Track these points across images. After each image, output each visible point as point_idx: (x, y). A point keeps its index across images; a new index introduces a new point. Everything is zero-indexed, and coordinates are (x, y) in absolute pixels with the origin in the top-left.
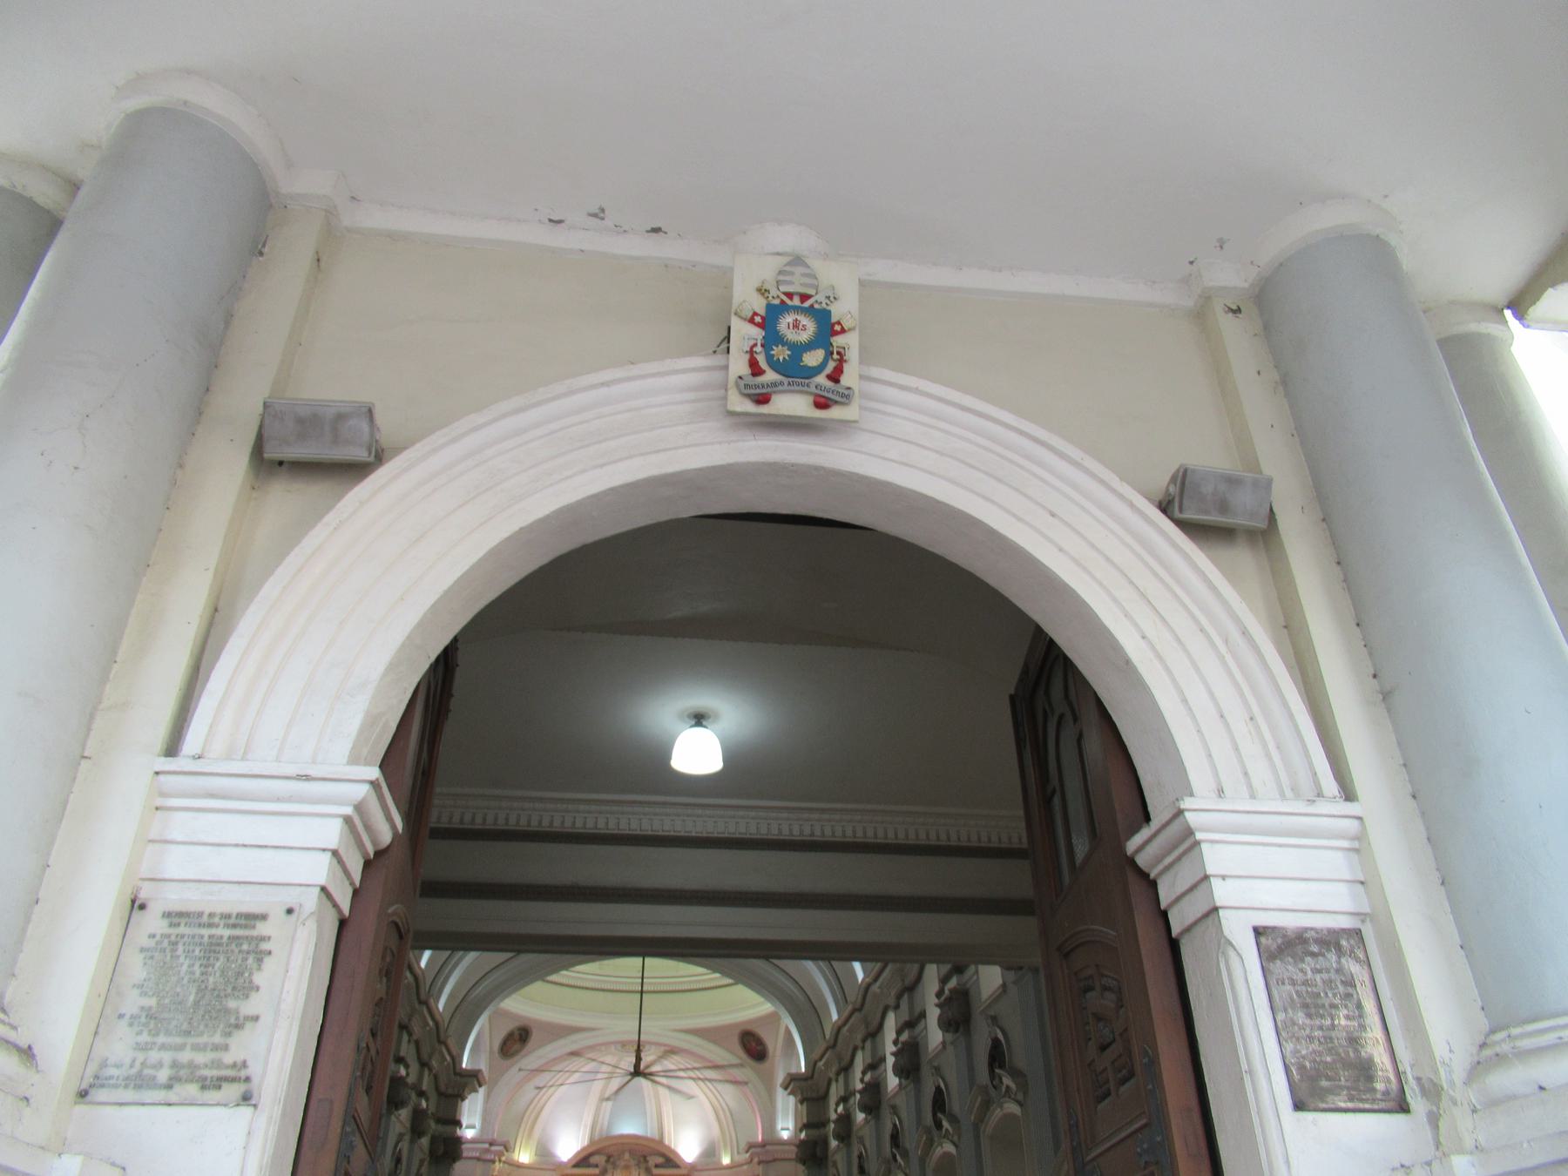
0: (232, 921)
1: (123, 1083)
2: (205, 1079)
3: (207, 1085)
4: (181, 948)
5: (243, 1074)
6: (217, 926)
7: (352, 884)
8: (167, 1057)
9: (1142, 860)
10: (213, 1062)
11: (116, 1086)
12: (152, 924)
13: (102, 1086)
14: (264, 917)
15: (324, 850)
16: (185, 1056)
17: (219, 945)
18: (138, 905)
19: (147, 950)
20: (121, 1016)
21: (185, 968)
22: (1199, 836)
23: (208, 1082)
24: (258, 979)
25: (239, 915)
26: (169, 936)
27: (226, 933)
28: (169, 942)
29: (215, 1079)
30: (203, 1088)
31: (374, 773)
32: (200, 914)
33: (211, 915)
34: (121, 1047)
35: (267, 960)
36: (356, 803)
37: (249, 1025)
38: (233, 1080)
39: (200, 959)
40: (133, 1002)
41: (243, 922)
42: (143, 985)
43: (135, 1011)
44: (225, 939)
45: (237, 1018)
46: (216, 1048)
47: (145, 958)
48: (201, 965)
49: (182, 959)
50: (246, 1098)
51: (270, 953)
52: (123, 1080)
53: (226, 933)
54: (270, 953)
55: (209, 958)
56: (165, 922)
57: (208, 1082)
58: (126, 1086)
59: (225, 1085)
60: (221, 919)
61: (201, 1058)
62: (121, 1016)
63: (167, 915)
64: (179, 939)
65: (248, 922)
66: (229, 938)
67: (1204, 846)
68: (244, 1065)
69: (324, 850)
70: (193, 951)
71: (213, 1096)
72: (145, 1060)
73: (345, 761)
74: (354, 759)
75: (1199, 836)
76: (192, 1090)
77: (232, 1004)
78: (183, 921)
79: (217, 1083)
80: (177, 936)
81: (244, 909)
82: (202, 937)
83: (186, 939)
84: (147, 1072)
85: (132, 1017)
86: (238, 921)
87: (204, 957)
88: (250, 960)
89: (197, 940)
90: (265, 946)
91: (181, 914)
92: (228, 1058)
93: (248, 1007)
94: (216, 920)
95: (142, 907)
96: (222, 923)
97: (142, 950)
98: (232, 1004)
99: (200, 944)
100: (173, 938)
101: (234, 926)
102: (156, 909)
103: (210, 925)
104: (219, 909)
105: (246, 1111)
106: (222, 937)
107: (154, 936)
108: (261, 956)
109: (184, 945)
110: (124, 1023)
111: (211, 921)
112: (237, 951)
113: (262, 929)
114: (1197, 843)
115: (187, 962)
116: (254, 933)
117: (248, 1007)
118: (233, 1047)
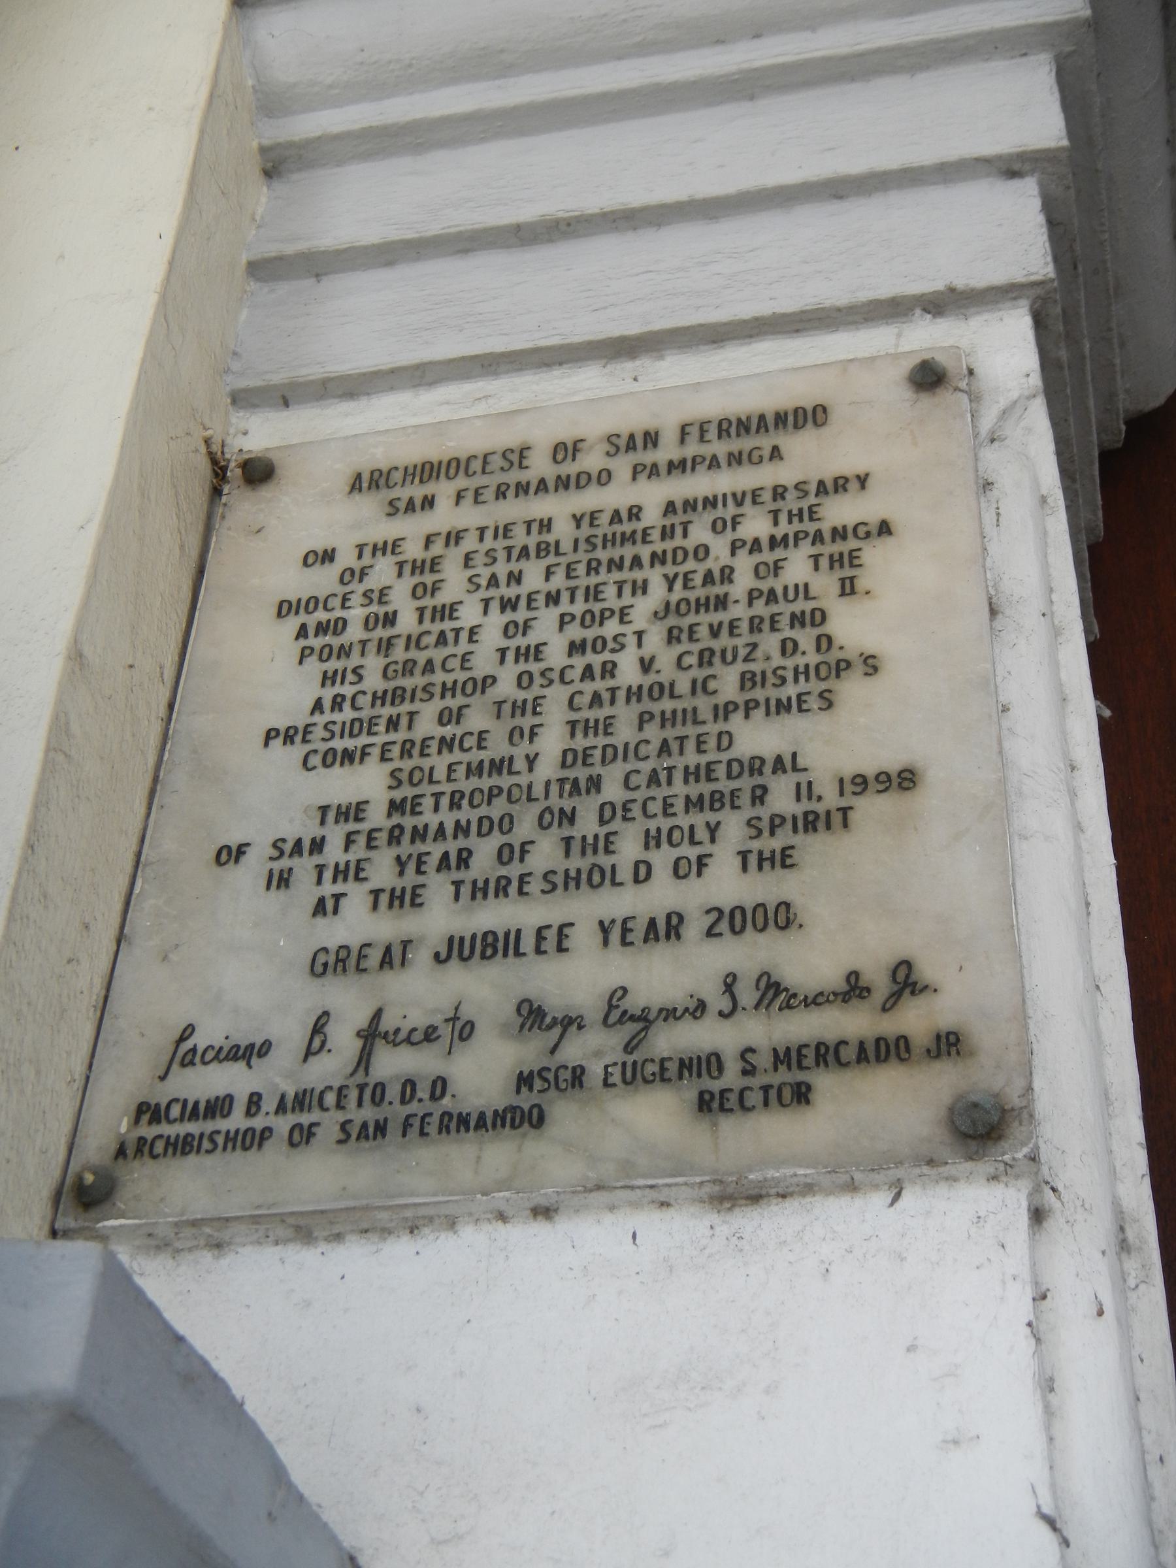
0: (668, 451)
1: (283, 1125)
2: (713, 1062)
6: (604, 478)
10: (730, 984)
11: (253, 1140)
13: (183, 1146)
19: (312, 603)
21: (492, 636)
26: (391, 547)
28: (401, 565)
29: (763, 1060)
30: (706, 1104)
32: (518, 456)
33: (566, 450)
35: (873, 554)
39: (553, 599)
41: (721, 448)
42: (307, 730)
44: (652, 517)
45: (804, 791)
47: (302, 632)
49: (469, 614)
52: (281, 1108)
54: (885, 529)
55: (593, 593)
56: (369, 505)
57: (731, 1077)
58: (302, 1136)
59: (824, 1082)
64: (437, 548)
65: (745, 444)
66: (670, 508)
70: (516, 578)
72: (378, 1014)
78: (444, 490)
80: (428, 541)
82: (546, 525)
83: (470, 543)
86: (692, 449)
87: (573, 591)
89: (519, 538)
91: (428, 471)
94: (592, 461)
97: (284, 609)
99: (542, 550)
100: (413, 550)
101: (678, 467)
103: (581, 481)
106: (635, 513)
107: (328, 556)
109: (468, 560)
112: (720, 547)
115: (496, 620)
116: (784, 474)
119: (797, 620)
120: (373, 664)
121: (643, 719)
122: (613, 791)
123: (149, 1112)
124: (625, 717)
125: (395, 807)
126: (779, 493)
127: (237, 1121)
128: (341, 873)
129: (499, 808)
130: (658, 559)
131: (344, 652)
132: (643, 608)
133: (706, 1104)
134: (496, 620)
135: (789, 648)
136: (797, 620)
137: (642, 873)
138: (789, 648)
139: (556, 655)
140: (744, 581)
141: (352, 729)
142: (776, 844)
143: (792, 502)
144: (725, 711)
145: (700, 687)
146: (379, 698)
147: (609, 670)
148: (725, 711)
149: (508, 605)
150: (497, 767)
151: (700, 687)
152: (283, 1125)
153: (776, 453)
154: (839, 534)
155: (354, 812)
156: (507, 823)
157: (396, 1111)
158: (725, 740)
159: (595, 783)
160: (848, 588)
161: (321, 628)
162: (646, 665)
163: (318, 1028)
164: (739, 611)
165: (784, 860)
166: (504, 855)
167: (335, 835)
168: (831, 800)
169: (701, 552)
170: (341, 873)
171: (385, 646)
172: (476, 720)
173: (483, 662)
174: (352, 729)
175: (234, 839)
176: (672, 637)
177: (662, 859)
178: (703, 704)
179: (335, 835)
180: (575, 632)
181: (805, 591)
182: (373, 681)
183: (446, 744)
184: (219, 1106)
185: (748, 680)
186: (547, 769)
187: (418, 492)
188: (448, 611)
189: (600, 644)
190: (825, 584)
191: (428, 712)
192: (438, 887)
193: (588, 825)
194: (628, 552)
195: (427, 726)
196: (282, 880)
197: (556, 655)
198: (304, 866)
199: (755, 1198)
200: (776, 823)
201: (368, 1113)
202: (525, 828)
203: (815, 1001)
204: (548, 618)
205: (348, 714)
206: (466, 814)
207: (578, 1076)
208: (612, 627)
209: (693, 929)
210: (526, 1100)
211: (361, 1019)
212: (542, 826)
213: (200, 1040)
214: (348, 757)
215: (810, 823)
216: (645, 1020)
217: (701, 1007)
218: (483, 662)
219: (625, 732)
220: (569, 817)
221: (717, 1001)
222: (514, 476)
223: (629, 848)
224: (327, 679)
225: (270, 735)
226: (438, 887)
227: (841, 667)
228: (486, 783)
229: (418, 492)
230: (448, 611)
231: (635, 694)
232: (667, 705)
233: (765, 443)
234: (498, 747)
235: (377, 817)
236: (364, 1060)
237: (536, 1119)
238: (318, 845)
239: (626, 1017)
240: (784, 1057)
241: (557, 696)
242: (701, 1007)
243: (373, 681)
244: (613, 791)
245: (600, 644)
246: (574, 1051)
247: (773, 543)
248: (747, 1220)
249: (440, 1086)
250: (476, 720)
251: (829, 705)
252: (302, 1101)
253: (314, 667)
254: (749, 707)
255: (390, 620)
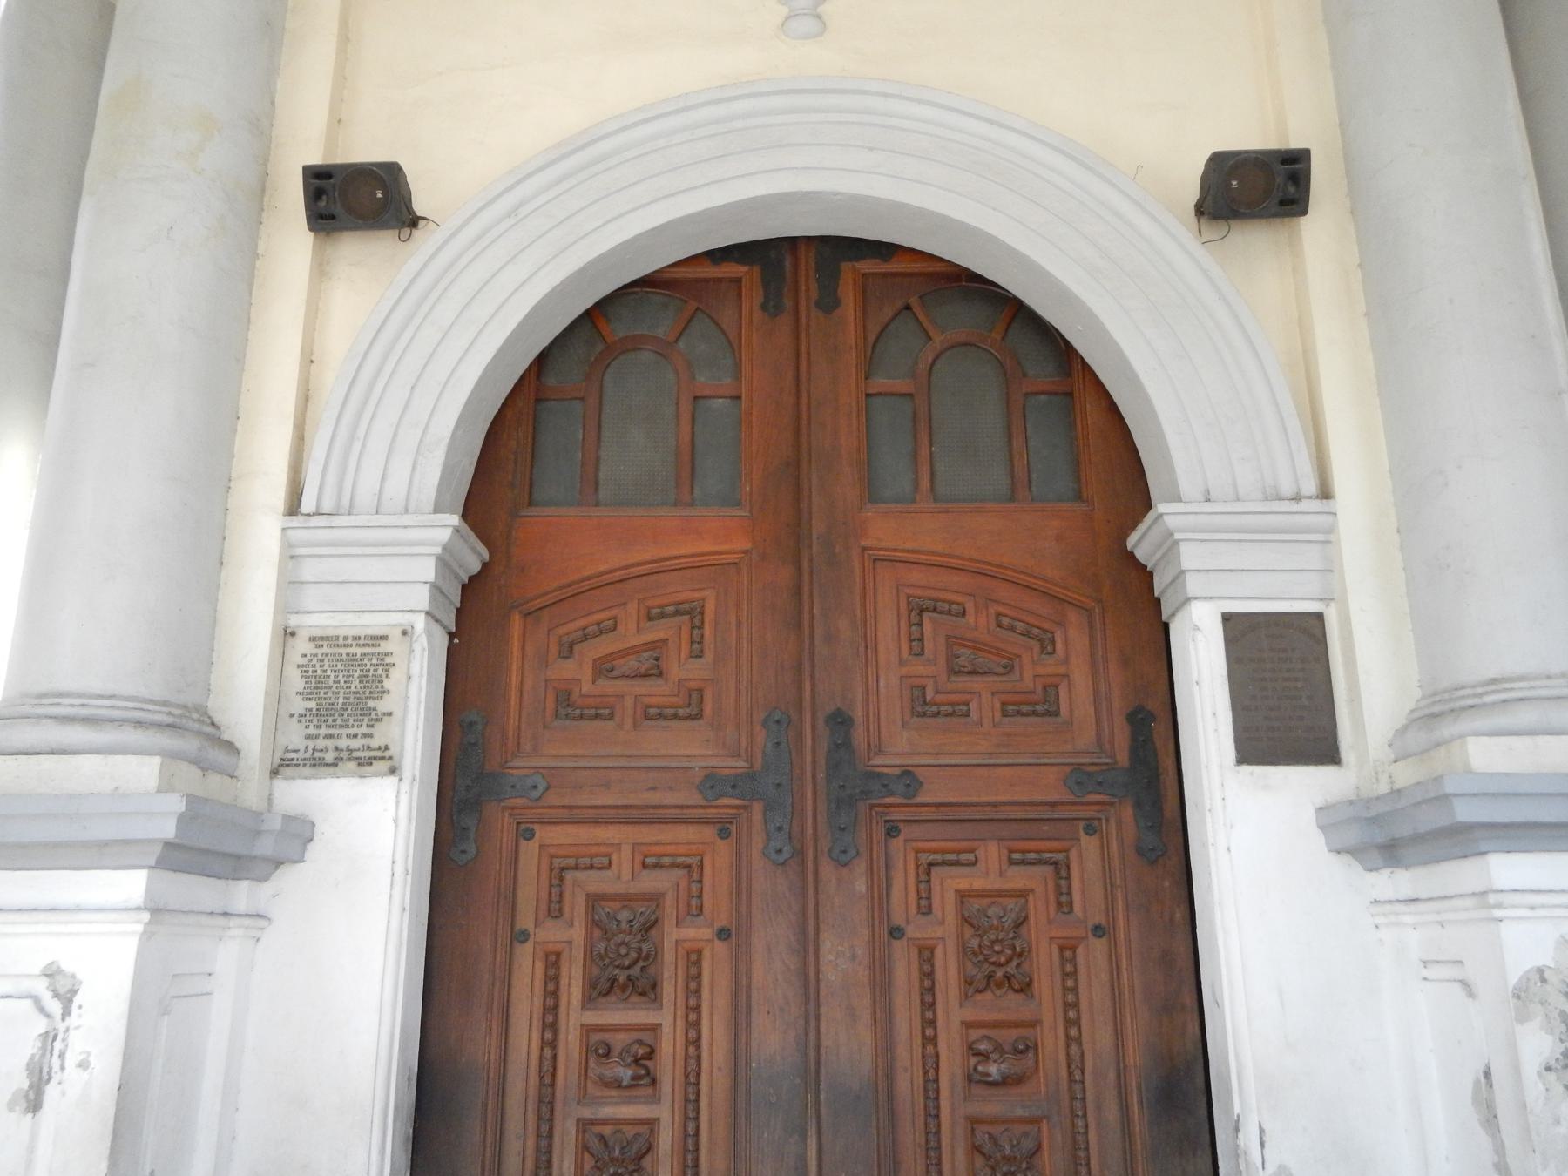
0: (362, 642)
3: (362, 763)
4: (326, 664)
5: (387, 754)
7: (451, 603)
8: (330, 743)
9: (1140, 555)
10: (363, 746)
12: (301, 646)
13: (288, 765)
14: (385, 638)
15: (426, 583)
16: (343, 743)
17: (355, 660)
18: (289, 633)
19: (303, 666)
20: (292, 716)
21: (332, 678)
22: (1177, 536)
23: (362, 761)
24: (387, 684)
25: (367, 637)
26: (316, 655)
27: (359, 651)
30: (359, 764)
31: (455, 520)
32: (337, 638)
33: (346, 638)
34: (295, 736)
35: (392, 670)
36: (443, 544)
37: (385, 718)
38: (382, 758)
39: (342, 671)
40: (299, 705)
41: (370, 642)
43: (303, 712)
44: (358, 656)
45: (376, 714)
46: (365, 736)
48: (344, 676)
49: (329, 673)
50: (393, 771)
51: (394, 665)
53: (359, 651)
55: (348, 671)
56: (312, 645)
57: (362, 761)
58: (305, 765)
60: (353, 640)
61: (355, 744)
62: (292, 716)
63: (312, 639)
65: (374, 642)
67: (1184, 548)
68: (386, 748)
69: (426, 583)
70: (336, 666)
71: (367, 769)
73: (431, 508)
74: (438, 509)
75: (1177, 536)
76: (352, 765)
77: (371, 704)
78: (325, 643)
79: (370, 761)
81: (370, 632)
83: (329, 657)
84: (317, 755)
85: (300, 716)
88: (380, 672)
89: (337, 657)
90: (388, 660)
91: (322, 638)
92: (374, 743)
93: (382, 706)
94: (349, 641)
95: (293, 634)
96: (354, 643)
97: (299, 666)
98: (371, 704)
100: (320, 657)
102: (303, 635)
103: (345, 646)
104: (352, 632)
105: (393, 779)
107: (306, 656)
108: (388, 667)
110: (295, 719)
111: (346, 643)
112: (369, 664)
113: (385, 647)
114: (1176, 543)
117: (382, 706)
118: (376, 735)
119: (379, 682)
120: (313, 681)
121: (355, 698)
122: (349, 711)
123: (282, 759)
124: (352, 696)
125: (317, 710)
126: (379, 654)
127: (295, 762)
128: (309, 721)
129: (332, 712)
130: (359, 665)
131: (309, 677)
132: (356, 675)
133: (359, 764)
134: (333, 675)
135: (377, 687)
136: (379, 682)
137: (353, 726)
138: (377, 687)
139: (342, 683)
140: (372, 673)
141: (311, 693)
142: (371, 723)
143: (380, 657)
144: (367, 698)
145: (363, 693)
146: (315, 688)
147: (350, 687)
148: (367, 698)
149: (335, 671)
150: (333, 704)
151: (363, 693)
152: (302, 763)
153: (379, 645)
154: (387, 665)
155: (311, 710)
156: (333, 715)
157: (318, 762)
158: (366, 703)
159: (347, 709)
160: (387, 676)
161: (305, 671)
162: (356, 687)
163: (306, 748)
164: (370, 678)
165: (372, 726)
166: (333, 721)
167: (308, 714)
168: (380, 717)
169: (366, 665)
170: (309, 721)
171: (315, 677)
172: (330, 695)
173: (331, 683)
174: (311, 693)
175: (293, 712)
176: (360, 682)
177: (356, 724)
178: (364, 696)
179: (308, 714)
180: (345, 679)
181: (380, 676)
182: (313, 684)
183: (325, 698)
184: (293, 759)
185: (371, 692)
186: (340, 706)
187: (320, 643)
188: (325, 671)
189: (348, 682)
190: (384, 675)
191: (322, 692)
192: (324, 725)
193: (345, 716)
194: (354, 663)
195: (322, 695)
196: (300, 721)
197: (342, 683)
198: (303, 719)
199: (365, 777)
200: (372, 719)
201: (313, 762)
202: (336, 716)
203: (374, 750)
204: (341, 674)
205: (309, 690)
206: (328, 712)
207: (342, 759)
208: (351, 679)
209: (359, 737)
210: (335, 762)
211: (312, 747)
212: (339, 715)
213: (289, 748)
214: (310, 699)
215: (377, 720)
216: (352, 751)
217: (359, 750)
218: (331, 683)
219: (352, 700)
220: (343, 715)
221: (362, 749)
222: (336, 643)
223: (351, 721)
224: (306, 683)
225: (297, 693)
226: (324, 725)
227: (384, 692)
228: (330, 707)
229: (320, 643)
230: (325, 671)
231: (354, 693)
232: (358, 695)
233: (378, 642)
234: (333, 701)
235: (314, 711)
236: (313, 753)
237: (337, 765)
238: (305, 715)
239: (349, 750)
240: (369, 758)
241: (342, 691)
242: (359, 750)
243: (313, 684)
244: (349, 711)
245: (348, 682)
246: (342, 755)
247: (377, 665)
248: (363, 780)
249: (324, 759)
250: (330, 695)
251: (381, 699)
252: (305, 759)
253: (304, 680)
254: (370, 698)
255: (316, 671)
